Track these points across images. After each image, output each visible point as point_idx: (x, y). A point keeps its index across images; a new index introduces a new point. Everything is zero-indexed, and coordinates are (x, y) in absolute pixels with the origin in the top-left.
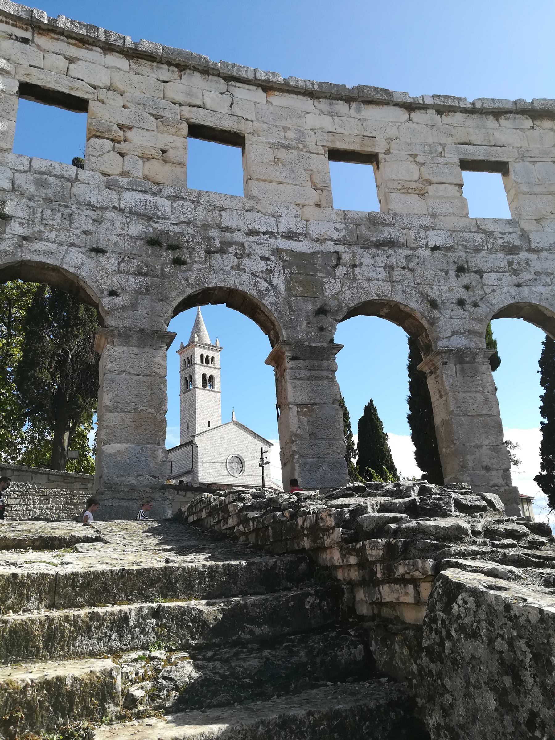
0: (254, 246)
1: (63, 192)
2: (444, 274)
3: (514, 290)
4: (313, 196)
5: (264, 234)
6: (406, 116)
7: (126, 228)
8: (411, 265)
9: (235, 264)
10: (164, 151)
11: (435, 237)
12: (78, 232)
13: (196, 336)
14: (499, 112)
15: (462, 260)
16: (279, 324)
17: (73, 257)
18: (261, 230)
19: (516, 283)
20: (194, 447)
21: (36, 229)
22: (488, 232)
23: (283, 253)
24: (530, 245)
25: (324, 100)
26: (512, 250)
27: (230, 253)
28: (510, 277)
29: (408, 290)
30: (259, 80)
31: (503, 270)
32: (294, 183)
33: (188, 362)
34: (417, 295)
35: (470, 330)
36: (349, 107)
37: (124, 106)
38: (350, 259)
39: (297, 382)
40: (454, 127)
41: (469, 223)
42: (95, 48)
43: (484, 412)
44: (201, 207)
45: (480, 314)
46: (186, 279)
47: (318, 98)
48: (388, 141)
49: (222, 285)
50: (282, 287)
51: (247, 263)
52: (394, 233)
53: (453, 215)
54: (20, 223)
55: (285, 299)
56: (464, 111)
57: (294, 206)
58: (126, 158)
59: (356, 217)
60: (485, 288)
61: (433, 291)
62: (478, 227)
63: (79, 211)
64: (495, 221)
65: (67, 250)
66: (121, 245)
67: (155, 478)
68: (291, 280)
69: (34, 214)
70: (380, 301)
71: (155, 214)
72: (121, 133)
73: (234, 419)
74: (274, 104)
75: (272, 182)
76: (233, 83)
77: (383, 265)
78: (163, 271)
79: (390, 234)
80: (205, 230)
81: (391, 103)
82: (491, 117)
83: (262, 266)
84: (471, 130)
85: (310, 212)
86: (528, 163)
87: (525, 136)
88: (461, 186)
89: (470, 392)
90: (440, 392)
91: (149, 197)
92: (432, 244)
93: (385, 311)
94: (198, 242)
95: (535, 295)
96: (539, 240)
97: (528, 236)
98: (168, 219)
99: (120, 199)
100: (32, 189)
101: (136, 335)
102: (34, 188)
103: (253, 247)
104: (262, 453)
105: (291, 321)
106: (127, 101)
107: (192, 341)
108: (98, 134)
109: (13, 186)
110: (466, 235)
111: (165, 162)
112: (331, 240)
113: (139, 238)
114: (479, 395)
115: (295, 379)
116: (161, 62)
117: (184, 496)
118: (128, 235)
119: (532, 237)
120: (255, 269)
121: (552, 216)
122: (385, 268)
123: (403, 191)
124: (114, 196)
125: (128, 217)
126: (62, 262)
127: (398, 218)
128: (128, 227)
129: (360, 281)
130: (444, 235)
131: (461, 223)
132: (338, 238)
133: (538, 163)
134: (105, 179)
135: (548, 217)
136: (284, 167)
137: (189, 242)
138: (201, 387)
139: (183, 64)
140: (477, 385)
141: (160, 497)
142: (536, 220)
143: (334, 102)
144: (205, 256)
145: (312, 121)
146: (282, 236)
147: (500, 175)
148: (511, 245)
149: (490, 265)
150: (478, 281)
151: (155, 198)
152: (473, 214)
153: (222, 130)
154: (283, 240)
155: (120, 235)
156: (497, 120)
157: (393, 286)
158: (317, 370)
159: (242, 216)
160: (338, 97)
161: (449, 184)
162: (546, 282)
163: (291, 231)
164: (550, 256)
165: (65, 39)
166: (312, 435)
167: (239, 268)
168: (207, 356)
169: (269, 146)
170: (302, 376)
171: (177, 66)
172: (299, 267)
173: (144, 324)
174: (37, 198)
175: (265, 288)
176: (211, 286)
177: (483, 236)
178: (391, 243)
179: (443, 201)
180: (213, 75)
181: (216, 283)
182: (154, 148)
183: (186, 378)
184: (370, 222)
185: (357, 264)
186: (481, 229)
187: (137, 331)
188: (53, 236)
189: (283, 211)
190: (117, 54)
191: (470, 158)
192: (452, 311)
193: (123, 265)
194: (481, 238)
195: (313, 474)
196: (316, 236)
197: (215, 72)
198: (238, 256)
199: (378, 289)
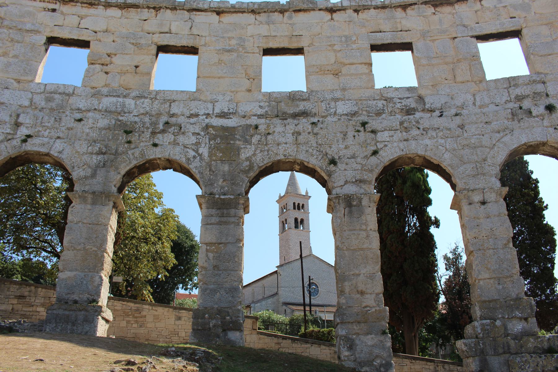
1: (63, 103)
2: (342, 136)
4: (246, 84)
7: (96, 123)
9: (172, 140)
11: (343, 106)
12: (63, 129)
14: (405, 5)
17: (58, 146)
19: (406, 138)
20: (279, 275)
21: (36, 130)
22: (389, 98)
23: (211, 129)
24: (425, 106)
25: (264, 14)
26: (409, 111)
29: (311, 150)
31: (395, 128)
32: (232, 76)
36: (283, 16)
37: (114, 41)
38: (265, 129)
39: (208, 226)
40: (368, 21)
41: (374, 93)
43: (365, 246)
46: (133, 154)
47: (259, 13)
48: (312, 37)
51: (181, 139)
52: (308, 106)
54: (27, 127)
55: (208, 163)
57: (229, 93)
61: (332, 149)
63: (71, 115)
64: (397, 89)
65: (54, 142)
66: (91, 134)
67: (92, 296)
69: (37, 120)
70: (287, 160)
72: (109, 59)
76: (194, 13)
77: (292, 131)
79: (304, 106)
81: (316, 9)
82: (399, 10)
86: (428, 42)
87: (427, 21)
89: (355, 230)
91: (120, 100)
92: (339, 111)
94: (147, 127)
95: (422, 147)
96: (432, 101)
100: (43, 104)
102: (44, 103)
103: (188, 127)
105: (210, 180)
106: (116, 37)
109: (31, 103)
115: (207, 224)
116: (143, 8)
118: (97, 127)
119: (426, 100)
120: (186, 142)
121: (446, 82)
122: (293, 134)
124: (95, 102)
125: (103, 115)
126: (50, 150)
127: (314, 94)
128: (97, 122)
129: (271, 145)
131: (368, 93)
132: (262, 113)
133: (437, 41)
134: (93, 91)
137: (140, 128)
139: (158, 6)
140: (362, 224)
141: (92, 310)
142: (432, 86)
143: (271, 14)
145: (251, 30)
148: (407, 108)
150: (373, 139)
152: (379, 85)
154: (217, 119)
155: (91, 128)
156: (405, 11)
157: (297, 147)
158: (226, 217)
160: (274, 10)
161: (359, 64)
163: (223, 112)
166: (216, 267)
168: (299, 204)
169: (216, 52)
170: (213, 221)
171: (154, 8)
172: (222, 138)
175: (192, 156)
176: (151, 157)
177: (384, 102)
178: (305, 114)
179: (352, 78)
180: (180, 9)
181: (155, 155)
182: (130, 65)
183: (283, 222)
185: (271, 132)
188: (46, 134)
189: (220, 98)
191: (379, 42)
192: (347, 164)
193: (90, 148)
194: (382, 104)
195: (213, 296)
196: (243, 113)
197: (181, 8)
198: (176, 134)
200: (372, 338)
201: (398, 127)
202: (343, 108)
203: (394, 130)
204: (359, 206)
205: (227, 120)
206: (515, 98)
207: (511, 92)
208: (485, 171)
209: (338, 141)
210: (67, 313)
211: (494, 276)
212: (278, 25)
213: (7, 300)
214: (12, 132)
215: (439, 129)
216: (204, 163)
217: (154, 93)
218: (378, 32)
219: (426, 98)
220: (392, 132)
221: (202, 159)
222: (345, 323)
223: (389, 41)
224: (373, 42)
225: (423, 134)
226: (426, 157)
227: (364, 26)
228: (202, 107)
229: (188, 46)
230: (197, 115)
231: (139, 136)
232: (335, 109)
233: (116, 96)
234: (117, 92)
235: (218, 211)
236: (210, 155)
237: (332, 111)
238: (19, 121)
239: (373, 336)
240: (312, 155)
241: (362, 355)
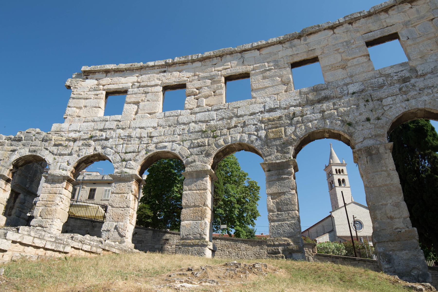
5: (258, 113)
6: (332, 32)
13: (331, 160)
15: (368, 96)
18: (256, 112)
19: (406, 99)
22: (387, 75)
24: (417, 73)
26: (405, 80)
28: (401, 97)
30: (254, 47)
33: (330, 175)
35: (375, 135)
36: (300, 40)
39: (271, 183)
40: (360, 27)
41: (374, 73)
42: (188, 64)
45: (382, 123)
47: (284, 43)
48: (322, 48)
51: (246, 129)
53: (364, 72)
56: (365, 17)
62: (381, 74)
64: (392, 67)
70: (319, 131)
72: (198, 91)
73: (353, 201)
74: (263, 54)
79: (325, 94)
82: (383, 13)
84: (371, 25)
86: (410, 28)
89: (377, 171)
92: (351, 91)
93: (327, 135)
96: (423, 68)
104: (354, 218)
107: (330, 163)
108: (189, 95)
110: (372, 80)
115: (270, 181)
119: (418, 69)
123: (332, 69)
127: (330, 84)
131: (370, 74)
135: (429, 53)
138: (338, 186)
139: (221, 54)
142: (420, 58)
143: (292, 41)
145: (280, 54)
146: (267, 112)
148: (403, 78)
150: (380, 105)
153: (239, 74)
156: (387, 13)
160: (293, 38)
161: (359, 57)
162: (428, 93)
164: (432, 76)
165: (178, 65)
168: (339, 170)
170: (273, 179)
171: (220, 56)
179: (356, 67)
180: (235, 53)
183: (330, 182)
186: (382, 74)
190: (197, 62)
191: (372, 39)
194: (383, 80)
200: (406, 253)
201: (399, 92)
203: (396, 95)
204: (378, 154)
205: (274, 113)
209: (353, 111)
212: (298, 47)
213: (158, 242)
215: (433, 87)
218: (369, 32)
219: (417, 67)
220: (394, 97)
222: (381, 242)
223: (379, 36)
225: (420, 93)
226: (427, 110)
227: (358, 31)
229: (243, 73)
232: (347, 91)
235: (276, 172)
239: (407, 251)
241: (400, 267)
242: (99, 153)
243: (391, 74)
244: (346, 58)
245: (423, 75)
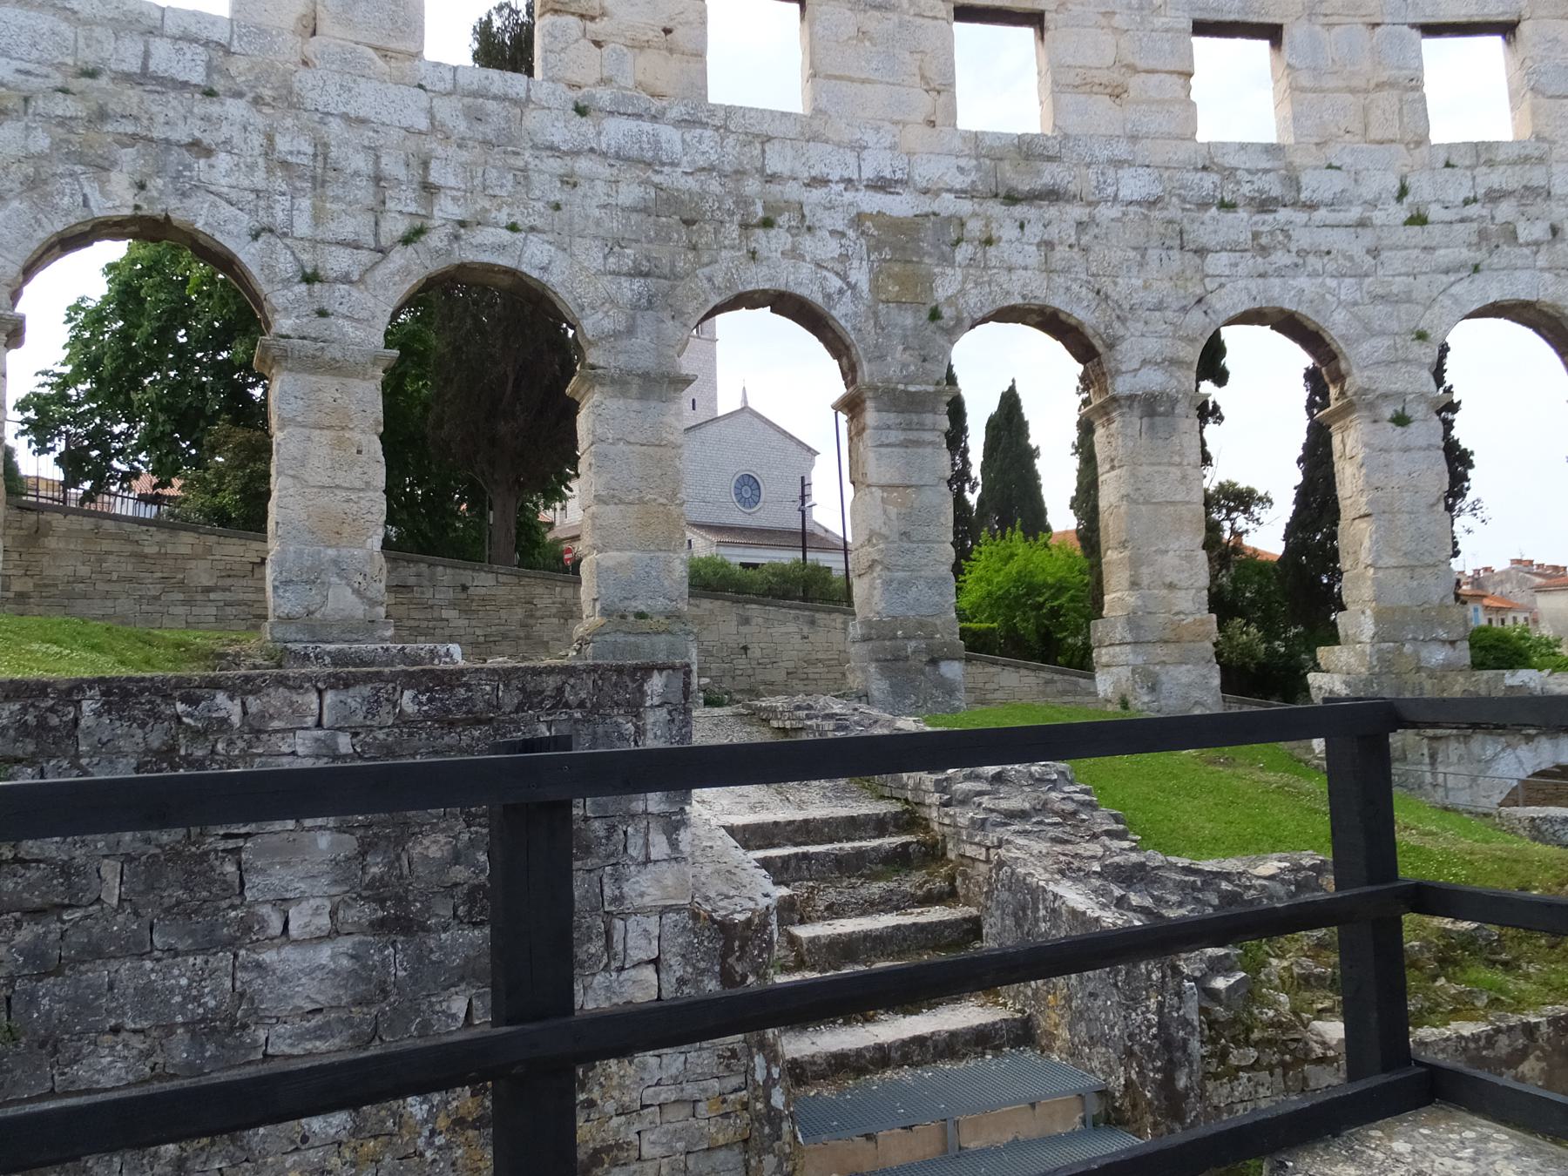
0: (820, 212)
1: (510, 128)
3: (1255, 285)
4: (924, 103)
7: (614, 194)
8: (1085, 239)
9: (788, 247)
10: (667, 31)
11: (1132, 181)
12: (539, 205)
16: (859, 350)
19: (1262, 271)
21: (478, 207)
22: (1226, 169)
23: (868, 224)
26: (1265, 205)
27: (780, 227)
29: (1075, 287)
31: (1243, 247)
32: (891, 80)
34: (1091, 295)
39: (883, 450)
43: (1178, 498)
44: (731, 140)
46: (710, 280)
49: (767, 287)
50: (864, 286)
51: (807, 243)
54: (453, 198)
55: (870, 307)
57: (888, 126)
58: (606, 50)
59: (997, 143)
60: (1207, 280)
64: (1243, 147)
65: (525, 239)
66: (607, 224)
68: (881, 272)
69: (472, 178)
71: (656, 156)
75: (852, 80)
78: (673, 266)
80: (738, 180)
83: (833, 248)
85: (915, 135)
86: (1318, 28)
88: (1190, 75)
89: (1160, 464)
90: (1112, 460)
91: (647, 126)
92: (1125, 193)
97: (1297, 178)
98: (677, 165)
99: (599, 134)
100: (462, 126)
101: (637, 380)
109: (432, 124)
110: (1188, 175)
111: (671, 51)
112: (949, 191)
113: (635, 210)
114: (1173, 469)
115: (880, 446)
117: (698, 606)
119: (1305, 179)
122: (1039, 245)
123: (1083, 89)
125: (612, 166)
130: (1147, 177)
131: (1181, 152)
132: (964, 186)
136: (874, 49)
142: (1317, 144)
144: (740, 236)
146: (867, 186)
147: (1266, 44)
149: (1221, 238)
151: (656, 126)
152: (1207, 132)
154: (870, 193)
155: (604, 207)
157: (1049, 279)
159: (800, 152)
161: (1167, 72)
162: (1314, 270)
166: (905, 535)
167: (795, 254)
170: (892, 439)
172: (894, 249)
173: (646, 362)
174: (470, 143)
176: (750, 288)
178: (1053, 195)
184: (1020, 153)
187: (638, 375)
189: (869, 137)
192: (1146, 323)
193: (611, 260)
196: (924, 184)
198: (794, 231)
199: (1025, 285)
200: (1188, 671)
202: (1133, 185)
205: (891, 197)
206: (1486, 194)
207: (1478, 180)
208: (1411, 357)
210: (632, 639)
211: (1405, 562)
214: (423, 212)
216: (862, 308)
217: (722, 114)
220: (1238, 254)
221: (856, 296)
224: (1199, 15)
228: (834, 160)
230: (822, 182)
231: (716, 232)
232: (1115, 188)
233: (633, 115)
234: (633, 105)
236: (875, 288)
237: (1110, 191)
238: (431, 179)
239: (1189, 666)
240: (1080, 300)
241: (1172, 702)
242: (167, 218)
243: (1238, 173)
244: (1130, 59)
245: (1311, 206)
